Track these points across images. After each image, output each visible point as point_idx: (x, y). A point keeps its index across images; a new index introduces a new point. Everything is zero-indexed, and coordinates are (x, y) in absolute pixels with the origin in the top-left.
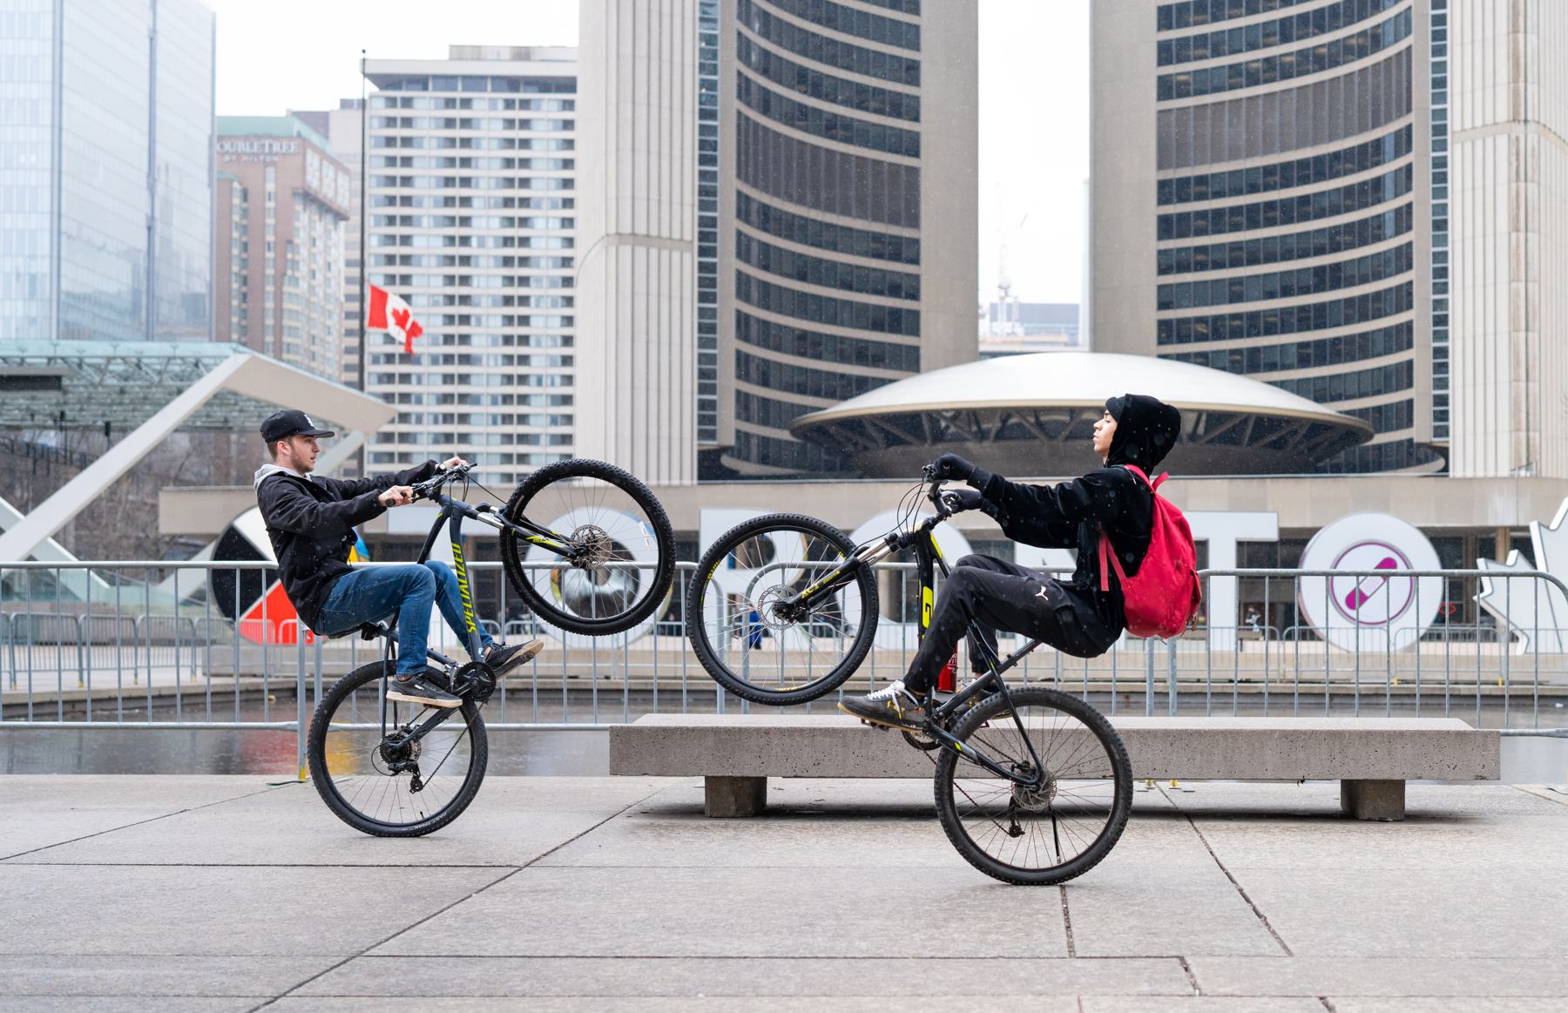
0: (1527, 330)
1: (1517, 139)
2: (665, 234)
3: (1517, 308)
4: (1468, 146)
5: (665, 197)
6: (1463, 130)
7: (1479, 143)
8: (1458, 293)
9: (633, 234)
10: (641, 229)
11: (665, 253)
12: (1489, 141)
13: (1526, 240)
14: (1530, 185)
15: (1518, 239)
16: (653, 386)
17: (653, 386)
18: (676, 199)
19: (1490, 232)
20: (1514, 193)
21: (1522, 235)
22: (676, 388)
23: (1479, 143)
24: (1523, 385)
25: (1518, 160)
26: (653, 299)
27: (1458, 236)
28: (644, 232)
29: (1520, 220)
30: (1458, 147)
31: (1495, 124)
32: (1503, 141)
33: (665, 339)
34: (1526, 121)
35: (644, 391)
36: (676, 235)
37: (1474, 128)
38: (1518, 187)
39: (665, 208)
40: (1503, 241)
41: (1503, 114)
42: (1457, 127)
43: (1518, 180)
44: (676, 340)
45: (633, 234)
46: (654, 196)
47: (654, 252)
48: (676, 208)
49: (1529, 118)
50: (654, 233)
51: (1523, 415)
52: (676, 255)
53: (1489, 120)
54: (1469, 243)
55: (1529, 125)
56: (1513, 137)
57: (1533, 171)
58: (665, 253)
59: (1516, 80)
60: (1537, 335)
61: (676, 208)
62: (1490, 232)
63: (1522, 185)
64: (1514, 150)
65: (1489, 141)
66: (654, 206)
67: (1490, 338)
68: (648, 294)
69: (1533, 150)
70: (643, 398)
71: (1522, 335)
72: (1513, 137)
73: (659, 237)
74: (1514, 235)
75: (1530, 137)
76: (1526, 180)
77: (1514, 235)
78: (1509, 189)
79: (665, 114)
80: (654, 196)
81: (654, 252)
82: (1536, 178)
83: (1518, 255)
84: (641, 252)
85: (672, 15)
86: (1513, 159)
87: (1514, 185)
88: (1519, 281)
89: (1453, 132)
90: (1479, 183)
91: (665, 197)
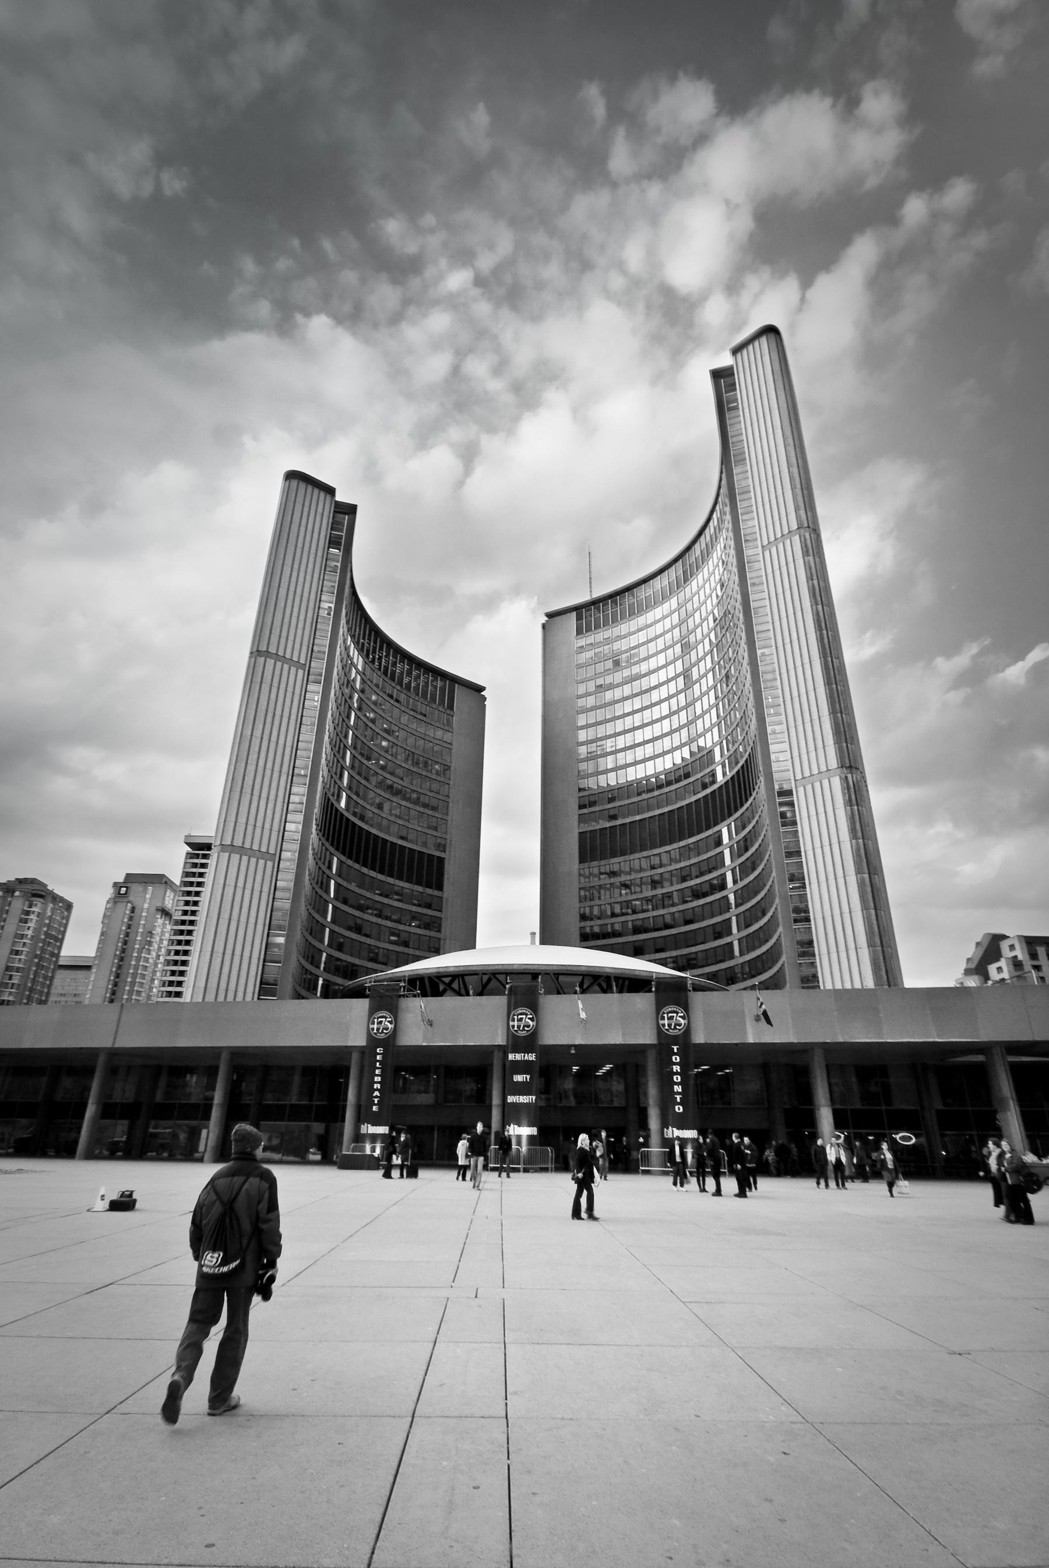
0: (876, 909)
1: (846, 777)
4: (809, 788)
5: (259, 824)
6: (804, 778)
7: (817, 785)
8: (815, 886)
9: (232, 845)
10: (238, 842)
12: (826, 782)
13: (864, 845)
15: (858, 844)
16: (229, 952)
17: (229, 952)
19: (835, 840)
21: (861, 841)
22: (247, 954)
23: (817, 785)
24: (880, 948)
27: (809, 847)
30: (801, 790)
31: (828, 770)
32: (836, 782)
33: (243, 919)
35: (220, 955)
37: (812, 775)
39: (258, 831)
41: (833, 763)
42: (799, 776)
43: (851, 805)
44: (252, 920)
45: (232, 845)
46: (251, 821)
47: (245, 858)
49: (852, 764)
50: (247, 845)
51: (883, 972)
52: (261, 862)
54: (818, 851)
56: (843, 776)
58: (253, 860)
62: (835, 840)
65: (826, 782)
67: (847, 916)
68: (236, 887)
70: (219, 960)
71: (873, 912)
73: (251, 849)
75: (854, 776)
76: (857, 805)
77: (854, 841)
78: (845, 810)
80: (251, 821)
81: (245, 858)
82: (863, 803)
84: (235, 857)
85: (282, 716)
86: (846, 791)
87: (848, 808)
89: (795, 780)
90: (821, 810)
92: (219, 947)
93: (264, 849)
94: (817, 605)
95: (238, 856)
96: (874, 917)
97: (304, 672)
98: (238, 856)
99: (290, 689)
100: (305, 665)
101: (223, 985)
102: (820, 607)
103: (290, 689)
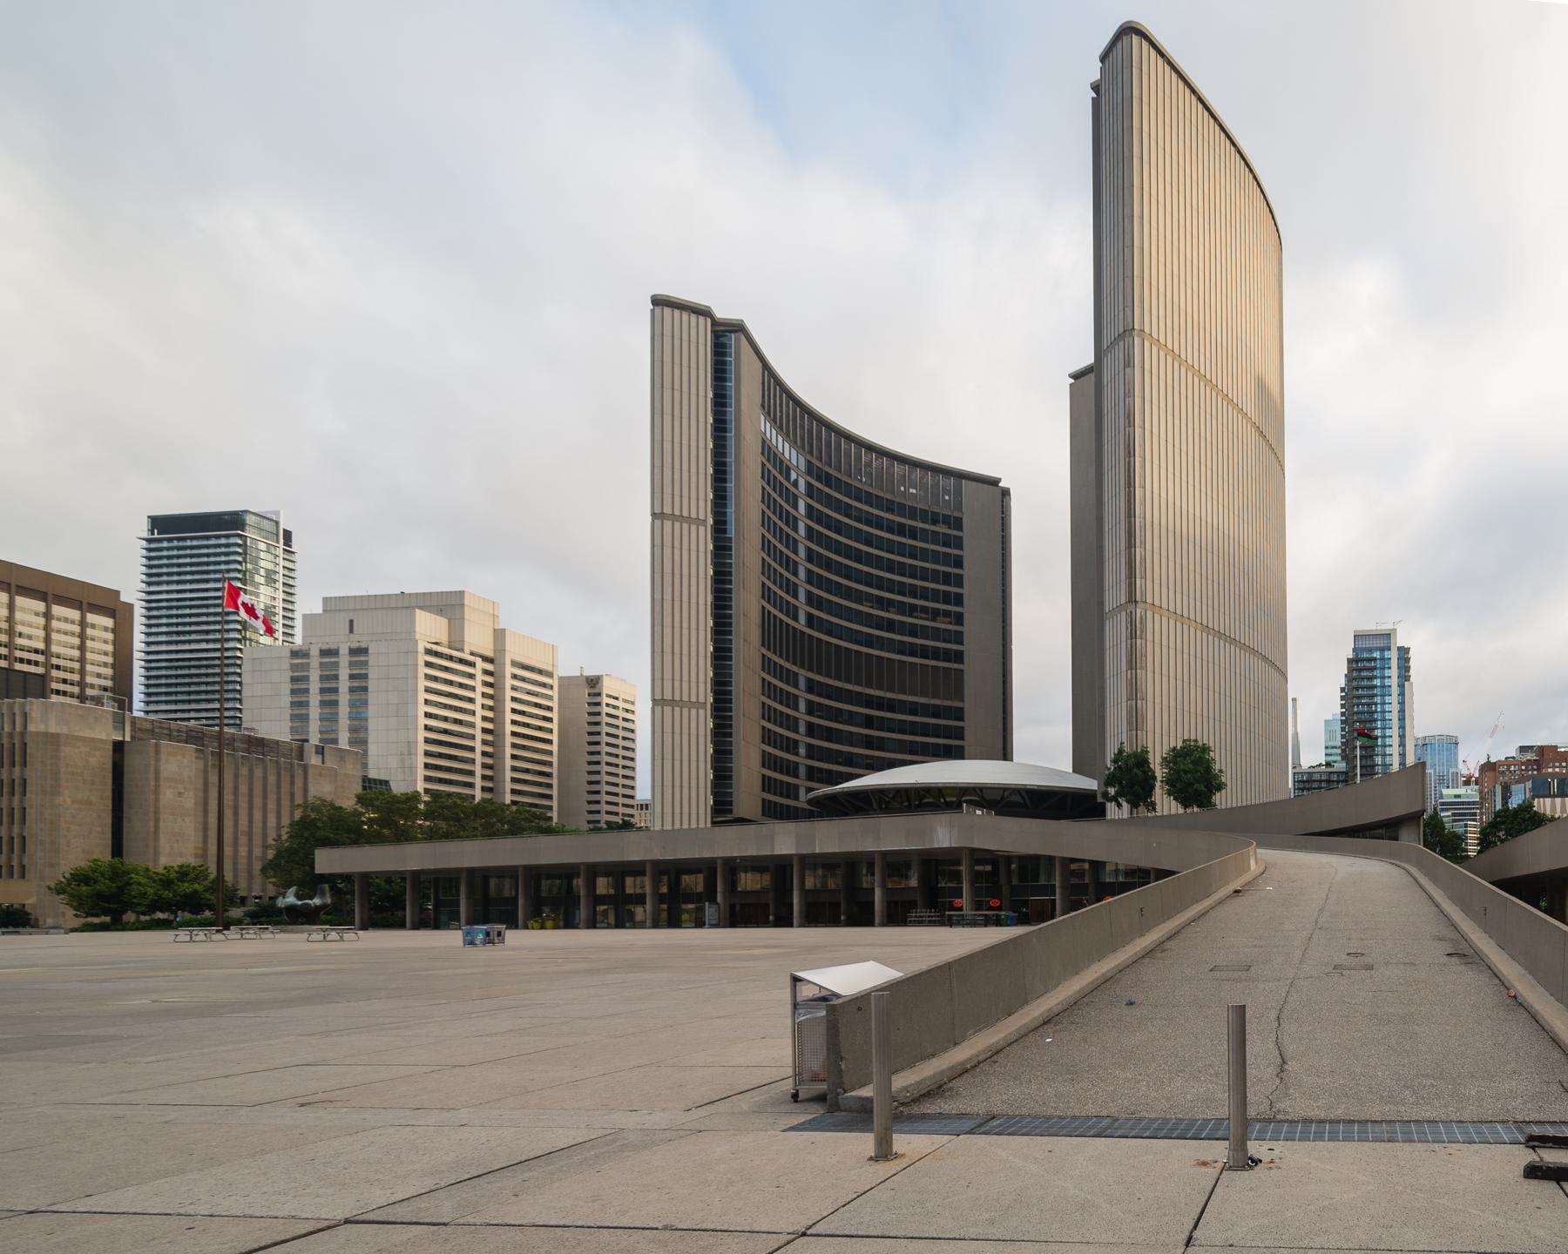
1: (1131, 612)
2: (685, 698)
3: (1131, 716)
5: (685, 678)
10: (668, 696)
11: (685, 710)
14: (1139, 641)
15: (1131, 673)
18: (693, 679)
20: (1129, 646)
21: (1134, 671)
25: (1131, 625)
26: (677, 737)
28: (660, 698)
29: (1132, 665)
30: (1107, 621)
32: (1124, 614)
33: (685, 758)
34: (1136, 602)
35: (670, 788)
36: (694, 699)
38: (1131, 642)
40: (1124, 675)
43: (1131, 639)
45: (663, 699)
46: (677, 677)
47: (677, 709)
48: (693, 685)
50: (677, 698)
53: (1118, 604)
55: (1139, 605)
56: (1128, 611)
57: (1142, 632)
59: (1130, 578)
60: (1145, 733)
61: (693, 685)
63: (1134, 640)
64: (1129, 620)
66: (677, 684)
68: (673, 733)
69: (1141, 617)
70: (670, 792)
71: (1134, 733)
72: (1128, 611)
74: (1129, 672)
79: (685, 632)
81: (677, 709)
82: (1144, 636)
83: (1132, 683)
84: (668, 710)
86: (1129, 626)
87: (1129, 641)
88: (1132, 700)
91: (685, 678)
92: (668, 782)
93: (694, 699)
94: (1130, 427)
95: (670, 708)
96: (1134, 738)
97: (706, 527)
98: (670, 708)
99: (693, 547)
100: (705, 520)
101: (677, 810)
102: (1131, 429)
103: (693, 547)
